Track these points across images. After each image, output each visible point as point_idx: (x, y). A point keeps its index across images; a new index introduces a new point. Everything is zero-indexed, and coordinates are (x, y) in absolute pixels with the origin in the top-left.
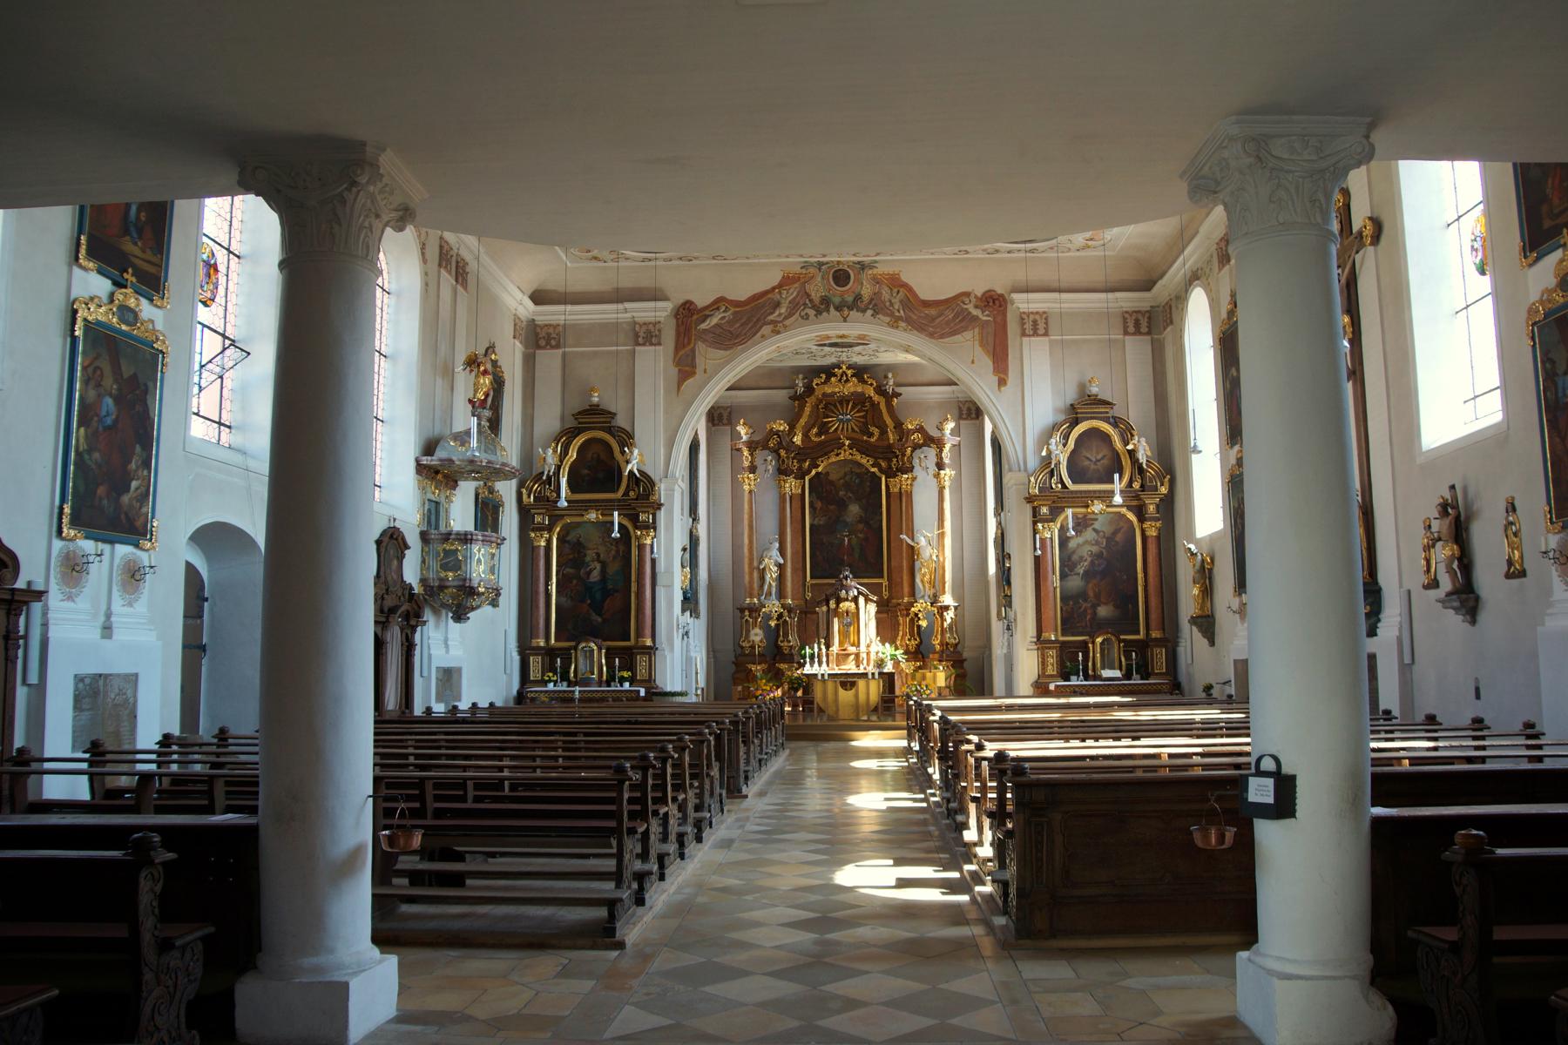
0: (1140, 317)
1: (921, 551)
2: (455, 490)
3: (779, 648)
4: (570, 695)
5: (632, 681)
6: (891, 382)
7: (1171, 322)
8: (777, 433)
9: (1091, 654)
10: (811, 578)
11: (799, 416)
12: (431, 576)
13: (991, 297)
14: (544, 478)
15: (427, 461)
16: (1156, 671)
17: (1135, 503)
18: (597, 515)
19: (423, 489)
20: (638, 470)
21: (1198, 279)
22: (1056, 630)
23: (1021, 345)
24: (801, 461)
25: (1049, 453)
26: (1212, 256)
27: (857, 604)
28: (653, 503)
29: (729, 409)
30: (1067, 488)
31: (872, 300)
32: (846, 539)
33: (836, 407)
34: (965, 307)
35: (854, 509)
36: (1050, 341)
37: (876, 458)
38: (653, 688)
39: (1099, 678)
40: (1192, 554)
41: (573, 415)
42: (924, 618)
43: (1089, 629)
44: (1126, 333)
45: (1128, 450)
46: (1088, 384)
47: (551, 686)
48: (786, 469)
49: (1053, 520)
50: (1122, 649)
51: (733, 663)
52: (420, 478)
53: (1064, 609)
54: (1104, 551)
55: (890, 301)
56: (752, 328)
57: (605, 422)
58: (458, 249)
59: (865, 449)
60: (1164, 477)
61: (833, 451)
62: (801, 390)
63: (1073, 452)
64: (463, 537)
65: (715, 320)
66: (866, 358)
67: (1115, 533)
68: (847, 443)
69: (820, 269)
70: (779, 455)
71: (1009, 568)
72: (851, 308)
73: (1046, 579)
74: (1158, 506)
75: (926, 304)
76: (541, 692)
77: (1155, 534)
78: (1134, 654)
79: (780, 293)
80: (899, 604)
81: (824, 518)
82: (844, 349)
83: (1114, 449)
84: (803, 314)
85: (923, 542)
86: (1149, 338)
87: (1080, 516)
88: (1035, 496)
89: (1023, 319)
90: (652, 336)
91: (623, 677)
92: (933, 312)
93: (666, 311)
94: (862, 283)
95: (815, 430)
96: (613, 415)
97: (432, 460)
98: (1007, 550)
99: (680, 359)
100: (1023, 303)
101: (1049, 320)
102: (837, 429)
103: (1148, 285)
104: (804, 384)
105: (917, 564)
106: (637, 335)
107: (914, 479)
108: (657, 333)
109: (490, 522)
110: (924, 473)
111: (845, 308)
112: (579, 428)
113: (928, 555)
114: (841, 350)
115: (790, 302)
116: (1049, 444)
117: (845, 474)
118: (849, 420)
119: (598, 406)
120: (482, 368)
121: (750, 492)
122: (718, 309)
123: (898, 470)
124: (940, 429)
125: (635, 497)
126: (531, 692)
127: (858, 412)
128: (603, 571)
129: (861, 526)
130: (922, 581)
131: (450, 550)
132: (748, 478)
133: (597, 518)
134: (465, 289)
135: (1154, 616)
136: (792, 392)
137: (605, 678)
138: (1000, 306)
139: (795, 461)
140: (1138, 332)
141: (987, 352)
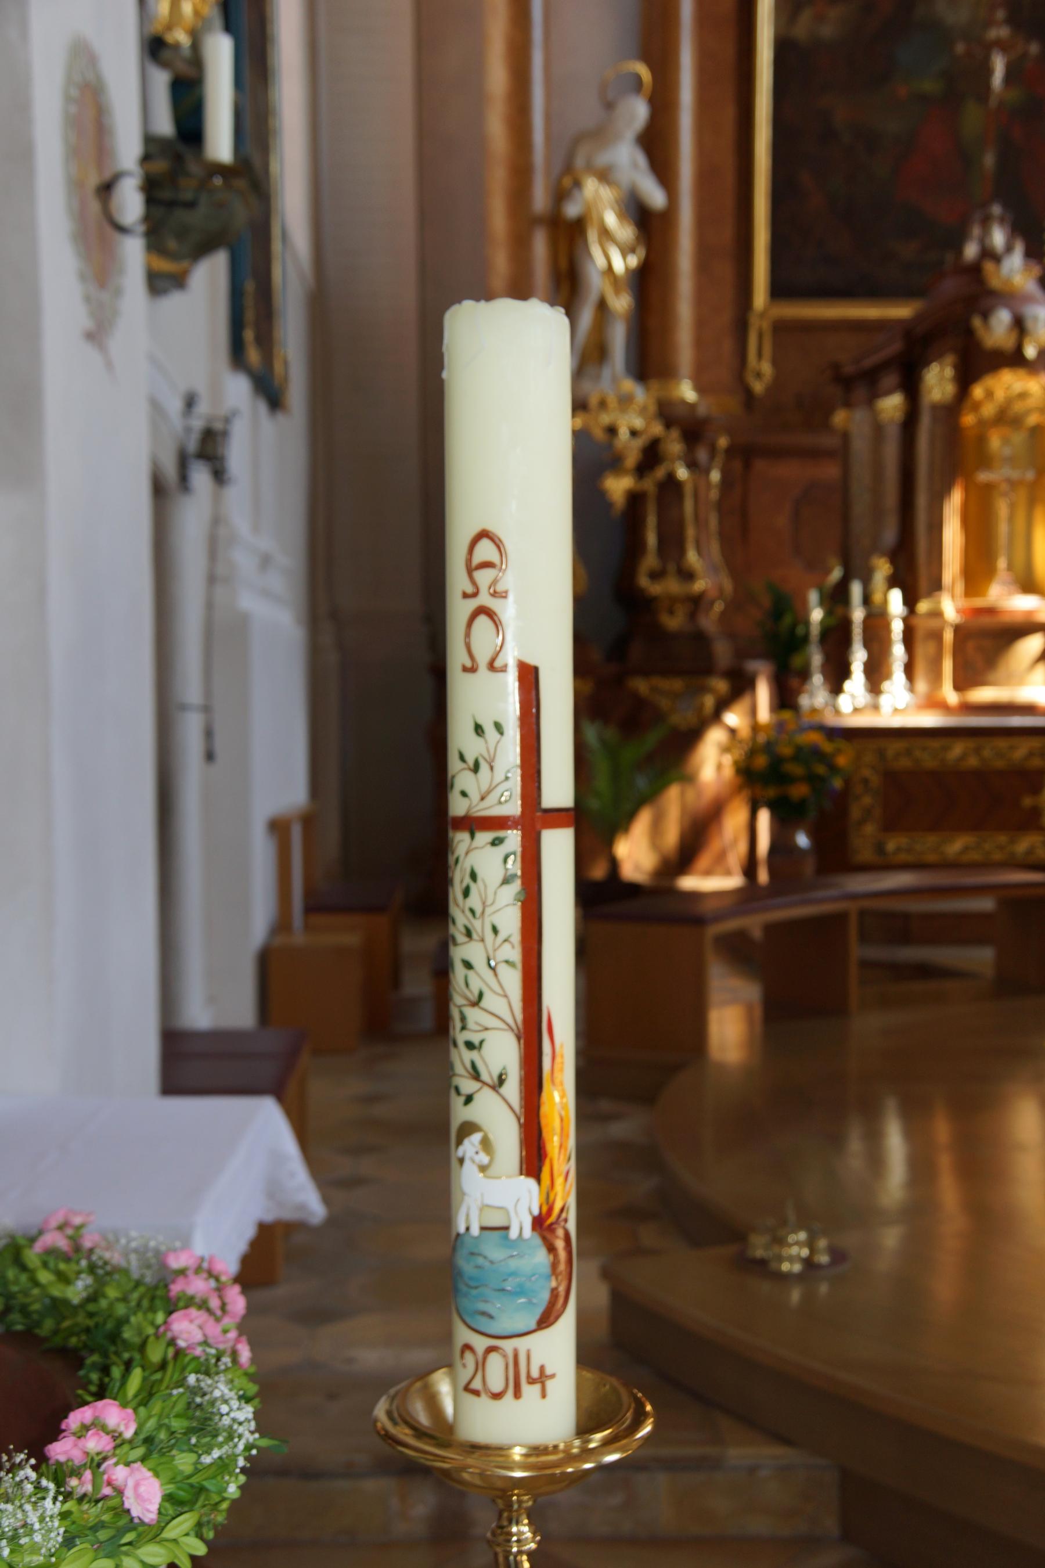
10: (779, 290)
32: (999, 66)
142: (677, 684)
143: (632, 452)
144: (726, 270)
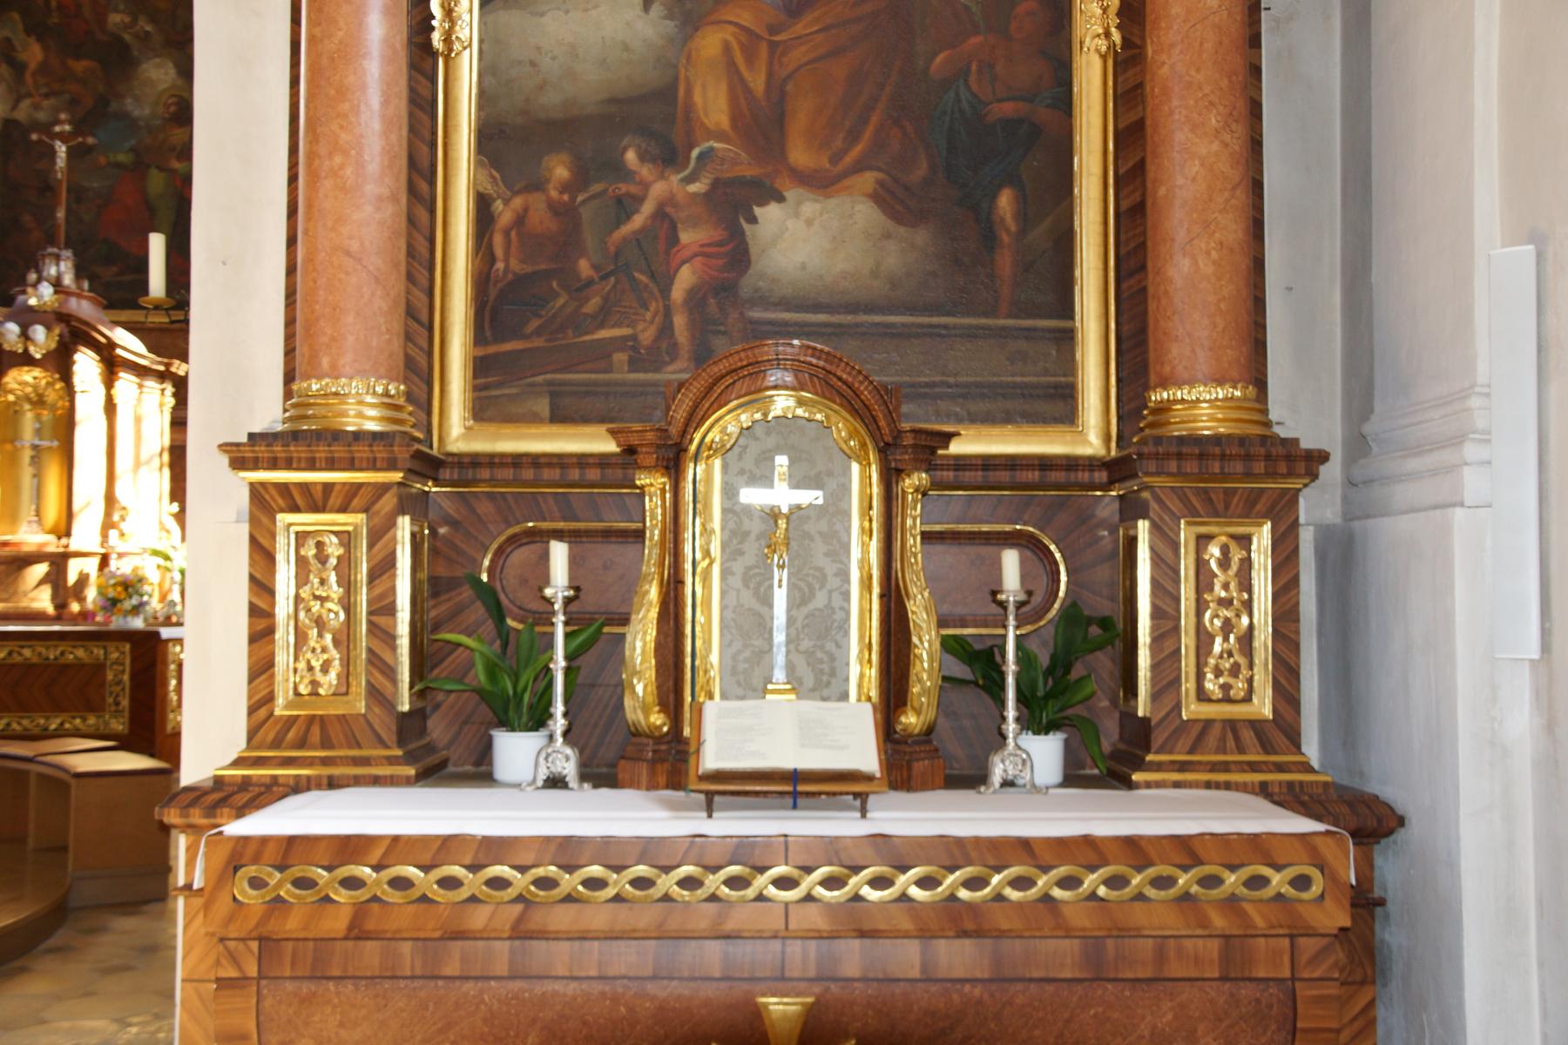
16: (1192, 710)
27: (66, 375)
32: (61, 149)
53: (504, 214)
78: (1011, 561)
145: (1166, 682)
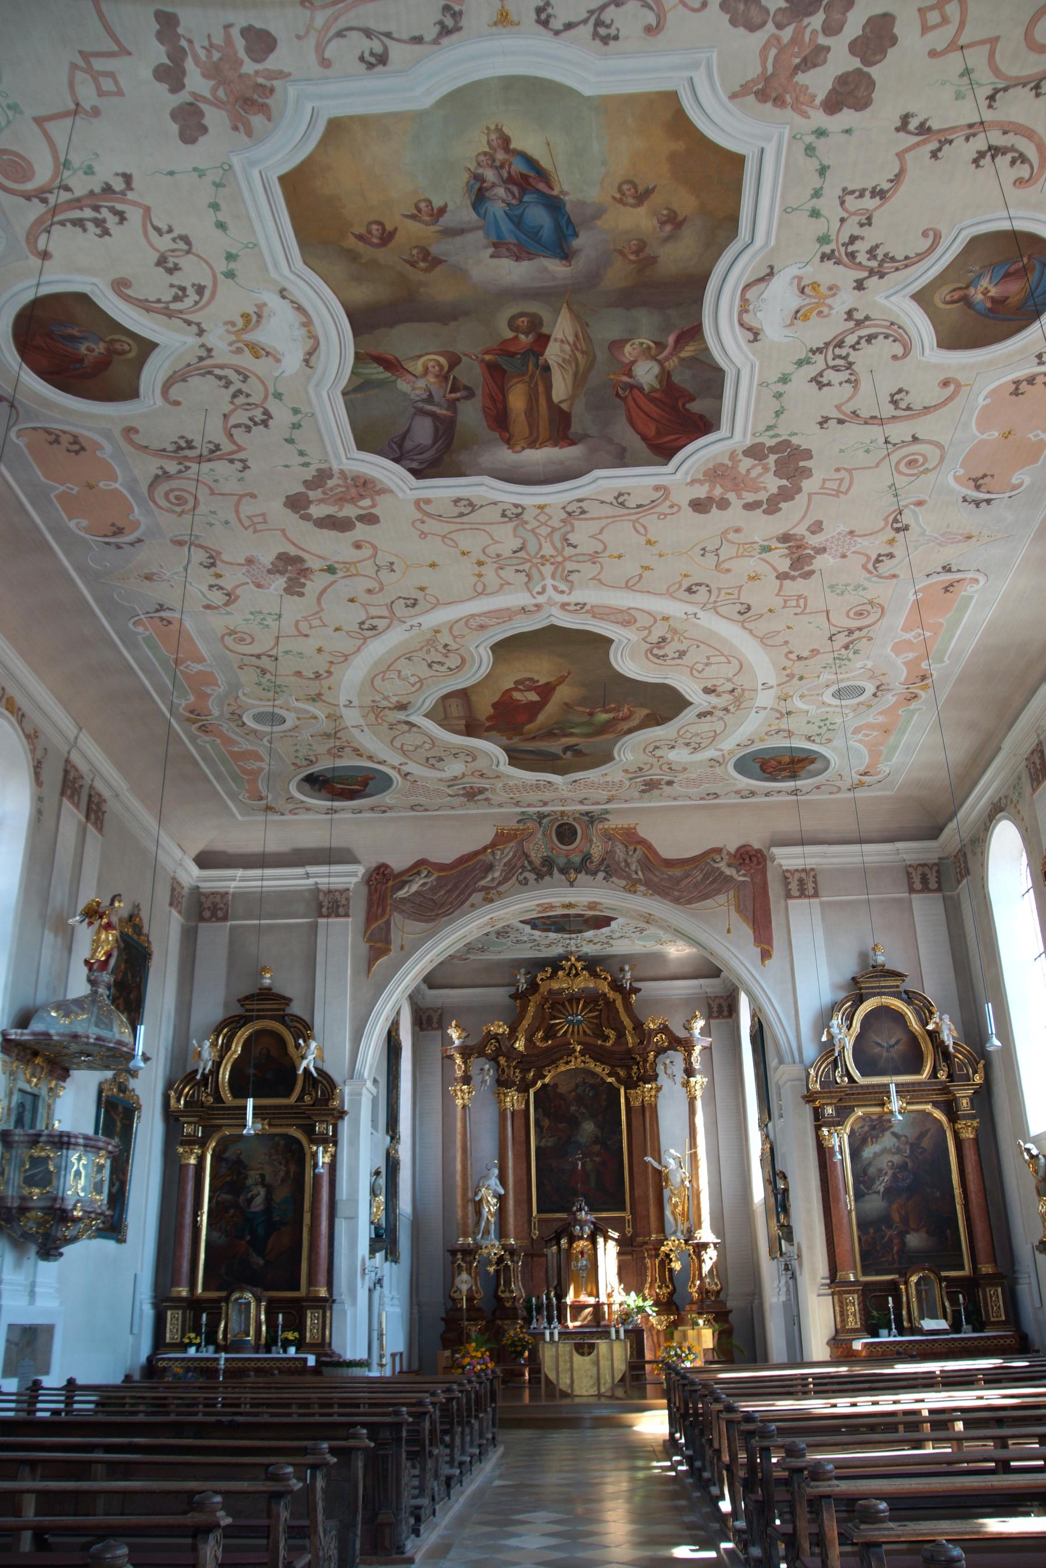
0: (926, 870)
1: (671, 1177)
2: (64, 1081)
3: (499, 1299)
4: (214, 1364)
5: (300, 1344)
6: (628, 976)
7: (968, 873)
8: (495, 1036)
9: (904, 1299)
10: (538, 1212)
11: (521, 1017)
12: (10, 1193)
13: (747, 852)
14: (198, 1077)
15: (16, 1034)
17: (941, 1098)
18: (263, 1124)
19: (12, 1075)
20: (316, 1069)
21: (1001, 810)
22: (855, 1268)
23: (787, 908)
24: (525, 1071)
25: (831, 1037)
26: (1019, 778)
27: (594, 1243)
28: (333, 1109)
29: (440, 1011)
30: (854, 1081)
31: (604, 860)
33: (564, 1006)
34: (716, 865)
35: (589, 1127)
36: (822, 904)
37: (613, 1066)
38: (326, 1355)
39: (920, 1331)
40: (1032, 1157)
41: (239, 1001)
42: (678, 1260)
43: (896, 1266)
44: (912, 890)
45: (928, 1031)
46: (871, 953)
47: (192, 1351)
48: (507, 1080)
49: (840, 1123)
50: (944, 1293)
51: (443, 1319)
52: (6, 1058)
53: (863, 1240)
54: (908, 1160)
55: (626, 861)
56: (458, 896)
57: (279, 1010)
58: (92, 780)
59: (599, 1055)
60: (978, 1063)
61: (562, 1058)
62: (523, 986)
63: (859, 1038)
64: (56, 1139)
65: (414, 888)
66: (598, 947)
67: (922, 1135)
68: (578, 1048)
69: (540, 823)
70: (498, 1063)
71: (786, 1191)
72: (578, 871)
73: (837, 1200)
74: (971, 1100)
75: (669, 863)
76: (176, 1359)
77: (972, 1136)
78: (961, 1296)
79: (493, 853)
80: (646, 1243)
81: (551, 1140)
82: (573, 936)
83: (911, 1031)
84: (521, 878)
85: (672, 1164)
86: (939, 895)
87: (874, 1117)
88: (816, 1093)
89: (786, 878)
90: (338, 907)
91: (286, 1339)
92: (678, 872)
93: (356, 876)
94: (591, 841)
95: (540, 1034)
96: (287, 1001)
97: (22, 1034)
98: (779, 1167)
99: (371, 934)
100: (788, 858)
101: (819, 878)
102: (566, 1032)
103: (934, 832)
104: (526, 980)
105: (666, 1193)
106: (320, 906)
107: (659, 1089)
108: (344, 902)
109: (118, 1129)
110: (670, 1081)
111: (572, 871)
112: (245, 1017)
113: (679, 1180)
114: (568, 936)
115: (505, 865)
116: (829, 1027)
117: (577, 1086)
118: (579, 1022)
119: (270, 989)
120: (105, 920)
121: (464, 1107)
122: (418, 873)
123: (639, 1079)
124: (688, 1028)
125: (311, 1102)
126: (163, 1359)
127: (590, 1011)
128: (269, 1199)
129: (597, 1148)
130: (673, 1213)
131: (39, 1158)
132: (461, 1090)
133: (263, 1129)
134: (100, 830)
135: (981, 1244)
136: (512, 990)
137: (263, 1341)
138: (759, 863)
139: (518, 1071)
140: (926, 888)
141: (745, 918)
142: (509, 1322)
143: (495, 1259)
144: (525, 1206)
145: (987, 1315)
